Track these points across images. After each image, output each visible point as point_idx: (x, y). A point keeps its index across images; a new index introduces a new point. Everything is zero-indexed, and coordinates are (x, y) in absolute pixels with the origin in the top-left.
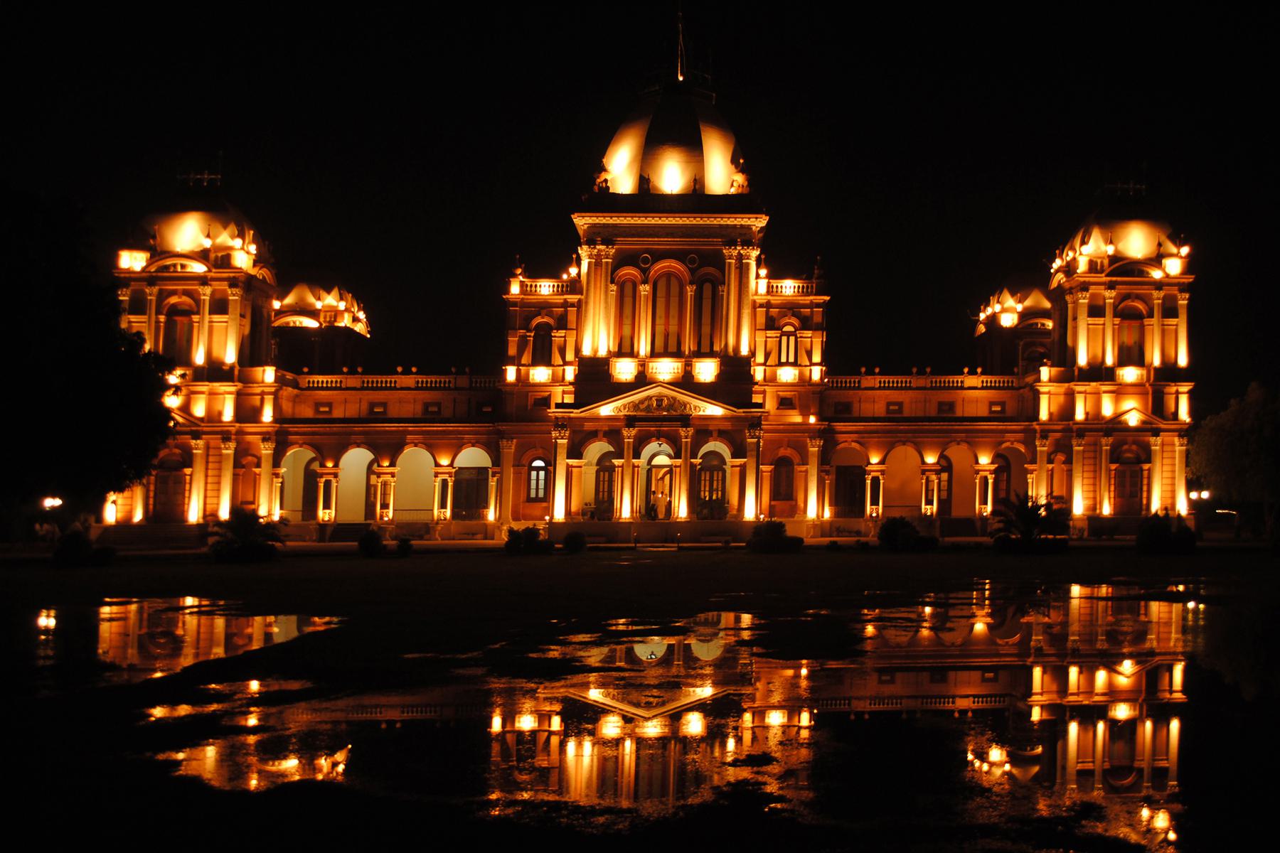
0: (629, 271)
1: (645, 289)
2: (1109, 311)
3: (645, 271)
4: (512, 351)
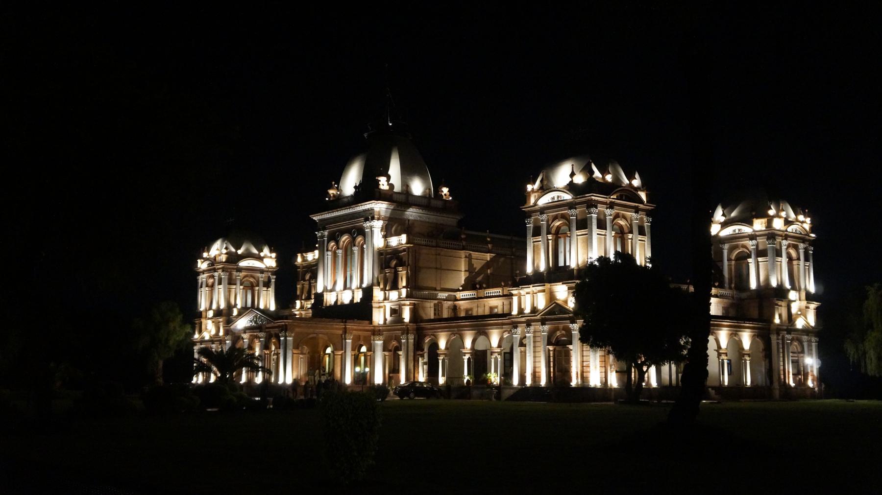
0: (332, 244)
1: (340, 252)
2: (544, 230)
3: (337, 243)
4: (298, 293)
